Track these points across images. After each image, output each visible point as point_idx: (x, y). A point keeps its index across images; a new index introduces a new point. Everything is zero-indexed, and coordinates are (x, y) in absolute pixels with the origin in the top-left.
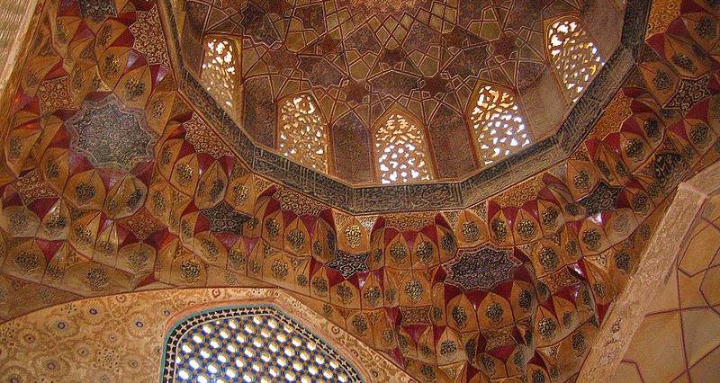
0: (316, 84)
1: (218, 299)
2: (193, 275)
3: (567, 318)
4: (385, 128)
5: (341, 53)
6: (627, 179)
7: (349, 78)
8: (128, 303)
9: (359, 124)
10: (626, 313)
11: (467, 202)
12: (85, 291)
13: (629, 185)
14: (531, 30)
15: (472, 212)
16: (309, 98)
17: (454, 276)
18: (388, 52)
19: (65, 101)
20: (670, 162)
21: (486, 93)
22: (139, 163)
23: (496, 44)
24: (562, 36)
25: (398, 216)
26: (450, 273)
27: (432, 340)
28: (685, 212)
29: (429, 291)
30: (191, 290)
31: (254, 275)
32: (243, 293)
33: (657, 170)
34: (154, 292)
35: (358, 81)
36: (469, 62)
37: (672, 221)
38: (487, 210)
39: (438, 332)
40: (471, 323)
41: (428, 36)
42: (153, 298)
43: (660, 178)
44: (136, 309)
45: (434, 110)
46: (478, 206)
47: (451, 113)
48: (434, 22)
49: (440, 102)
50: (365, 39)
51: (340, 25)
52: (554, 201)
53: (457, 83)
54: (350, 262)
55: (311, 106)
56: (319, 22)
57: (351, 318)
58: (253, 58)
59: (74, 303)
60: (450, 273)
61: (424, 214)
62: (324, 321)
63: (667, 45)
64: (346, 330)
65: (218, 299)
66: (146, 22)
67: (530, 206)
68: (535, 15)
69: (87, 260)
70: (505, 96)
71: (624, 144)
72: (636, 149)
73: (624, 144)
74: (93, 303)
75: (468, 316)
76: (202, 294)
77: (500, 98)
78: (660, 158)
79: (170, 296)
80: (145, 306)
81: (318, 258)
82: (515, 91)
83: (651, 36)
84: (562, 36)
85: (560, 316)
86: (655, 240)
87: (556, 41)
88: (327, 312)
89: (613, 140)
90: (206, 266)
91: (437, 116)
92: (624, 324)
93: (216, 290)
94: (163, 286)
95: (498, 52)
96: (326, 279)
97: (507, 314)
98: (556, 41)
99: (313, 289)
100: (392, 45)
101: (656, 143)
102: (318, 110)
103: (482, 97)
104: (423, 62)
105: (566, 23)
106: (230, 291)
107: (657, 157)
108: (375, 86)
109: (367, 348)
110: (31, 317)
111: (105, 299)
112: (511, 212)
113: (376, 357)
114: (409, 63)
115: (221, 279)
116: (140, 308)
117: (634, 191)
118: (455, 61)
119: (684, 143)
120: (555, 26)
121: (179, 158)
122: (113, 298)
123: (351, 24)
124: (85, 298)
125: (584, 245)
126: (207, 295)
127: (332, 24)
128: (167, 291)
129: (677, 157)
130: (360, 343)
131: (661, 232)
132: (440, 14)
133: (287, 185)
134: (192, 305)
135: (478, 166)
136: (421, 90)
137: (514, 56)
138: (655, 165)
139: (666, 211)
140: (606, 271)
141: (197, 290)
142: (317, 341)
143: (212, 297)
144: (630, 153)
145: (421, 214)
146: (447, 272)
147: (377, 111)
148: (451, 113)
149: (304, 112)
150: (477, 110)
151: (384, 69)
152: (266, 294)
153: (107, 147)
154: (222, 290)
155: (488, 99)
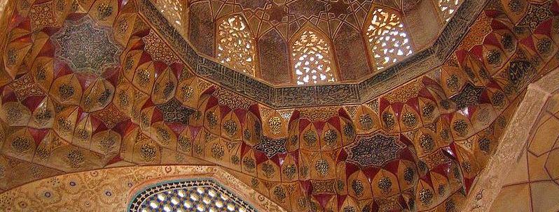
0: (246, 7)
1: (170, 174)
2: (151, 155)
3: (441, 189)
4: (300, 41)
6: (488, 81)
7: (272, 3)
8: (99, 177)
9: (279, 38)
10: (487, 184)
11: (364, 99)
12: (66, 167)
13: (489, 85)
16: (240, 18)
17: (353, 157)
19: (51, 21)
20: (522, 68)
21: (379, 14)
22: (108, 69)
25: (310, 110)
27: (336, 206)
28: (533, 106)
29: (334, 168)
30: (148, 167)
31: (197, 154)
32: (189, 170)
33: (512, 74)
34: (120, 169)
35: (279, 5)
37: (523, 113)
38: (379, 105)
39: (341, 200)
40: (367, 193)
42: (119, 173)
43: (514, 80)
44: (106, 182)
45: (338, 28)
46: (372, 102)
47: (351, 30)
49: (343, 21)
52: (431, 98)
53: (355, 6)
54: (272, 145)
55: (242, 25)
57: (273, 189)
59: (58, 177)
60: (350, 154)
61: (330, 108)
62: (252, 191)
64: (269, 198)
65: (170, 174)
67: (413, 102)
69: (68, 144)
70: (393, 16)
71: (486, 54)
72: (495, 57)
73: (486, 54)
74: (72, 177)
75: (365, 187)
76: (157, 171)
77: (389, 18)
78: (514, 64)
79: (132, 171)
80: (113, 179)
81: (247, 142)
82: (401, 13)
85: (436, 187)
86: (510, 128)
88: (254, 184)
89: (478, 51)
90: (161, 149)
91: (340, 32)
92: (486, 194)
93: (168, 167)
94: (127, 164)
96: (254, 158)
97: (395, 186)
99: (243, 166)
101: (511, 54)
102: (248, 27)
103: (375, 17)
106: (179, 167)
107: (511, 64)
110: (25, 188)
111: (81, 174)
112: (398, 107)
115: (172, 159)
116: (109, 181)
117: (494, 90)
119: (533, 53)
121: (138, 66)
124: (66, 173)
125: (454, 132)
128: (130, 168)
129: (526, 64)
130: (280, 208)
131: (515, 122)
133: (223, 86)
134: (149, 179)
135: (372, 70)
136: (327, 12)
138: (510, 70)
139: (518, 106)
140: (472, 153)
141: (154, 167)
142: (247, 207)
143: (165, 172)
144: (491, 61)
145: (327, 108)
146: (348, 153)
147: (294, 28)
148: (351, 30)
149: (237, 29)
150: (371, 28)
152: (207, 170)
154: (173, 167)
155: (380, 19)
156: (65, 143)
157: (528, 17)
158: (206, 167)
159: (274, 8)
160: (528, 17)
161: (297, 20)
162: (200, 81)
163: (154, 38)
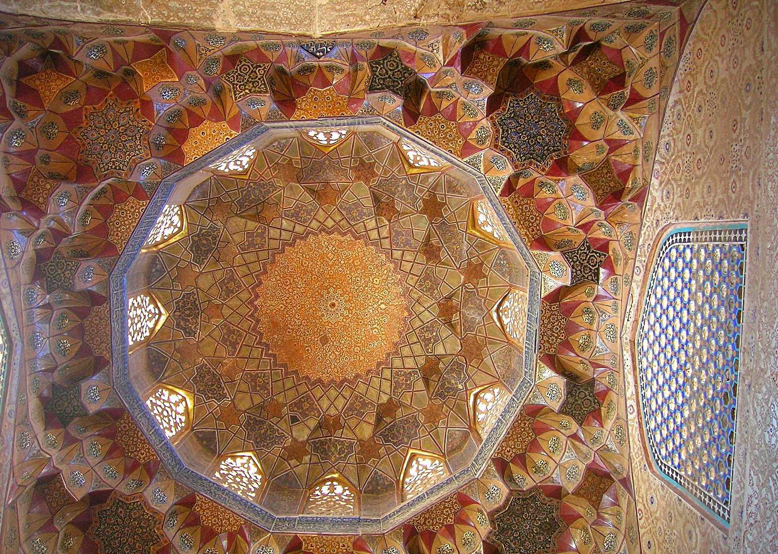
5: (449, 298)
7: (463, 285)
8: (643, 509)
9: (499, 258)
14: (340, 158)
15: (482, 168)
16: (501, 309)
17: (554, 151)
18: (428, 259)
21: (416, 161)
22: (547, 496)
23: (367, 181)
24: (328, 135)
26: (552, 158)
27: (625, 148)
28: (340, 10)
30: (631, 439)
35: (462, 277)
36: (399, 189)
41: (398, 233)
46: (473, 165)
48: (385, 233)
49: (445, 195)
50: (428, 284)
51: (426, 309)
53: (421, 191)
55: (504, 306)
56: (430, 329)
58: (479, 377)
60: (552, 158)
61: (509, 209)
62: (634, 285)
63: (232, 114)
66: (424, 523)
68: (327, 162)
69: (625, 541)
76: (633, 426)
80: (643, 491)
83: (234, 132)
84: (328, 135)
87: (335, 136)
88: (629, 281)
90: (618, 418)
91: (459, 192)
95: (374, 174)
98: (335, 136)
100: (422, 258)
104: (421, 226)
105: (315, 138)
106: (628, 394)
108: (461, 256)
109: (643, 232)
111: (642, 531)
113: (647, 222)
114: (428, 238)
118: (404, 200)
120: (326, 143)
122: (641, 522)
123: (421, 300)
126: (633, 420)
127: (427, 317)
130: (641, 243)
131: (366, 23)
132: (376, 231)
137: (369, 159)
139: (345, 33)
151: (444, 256)
153: (540, 527)
154: (629, 403)
156: (623, 546)
157: (253, 89)
158: (625, 352)
159: (468, 279)
160: (253, 89)
161: (471, 246)
162: (539, 378)
163: (502, 450)
